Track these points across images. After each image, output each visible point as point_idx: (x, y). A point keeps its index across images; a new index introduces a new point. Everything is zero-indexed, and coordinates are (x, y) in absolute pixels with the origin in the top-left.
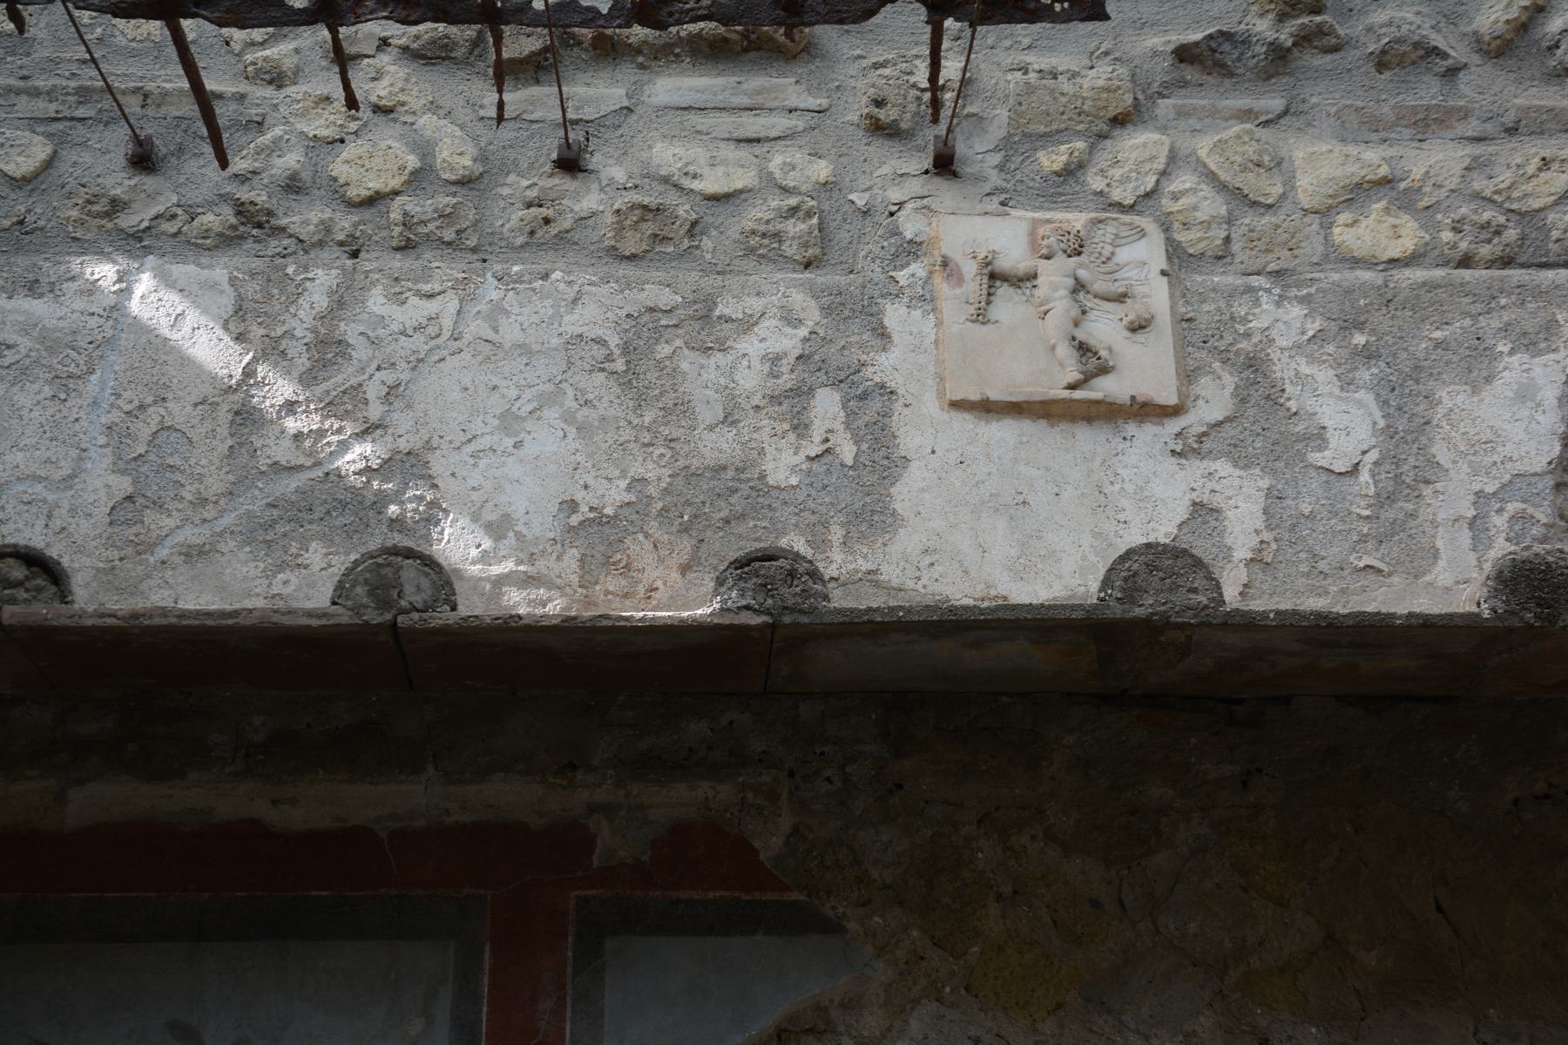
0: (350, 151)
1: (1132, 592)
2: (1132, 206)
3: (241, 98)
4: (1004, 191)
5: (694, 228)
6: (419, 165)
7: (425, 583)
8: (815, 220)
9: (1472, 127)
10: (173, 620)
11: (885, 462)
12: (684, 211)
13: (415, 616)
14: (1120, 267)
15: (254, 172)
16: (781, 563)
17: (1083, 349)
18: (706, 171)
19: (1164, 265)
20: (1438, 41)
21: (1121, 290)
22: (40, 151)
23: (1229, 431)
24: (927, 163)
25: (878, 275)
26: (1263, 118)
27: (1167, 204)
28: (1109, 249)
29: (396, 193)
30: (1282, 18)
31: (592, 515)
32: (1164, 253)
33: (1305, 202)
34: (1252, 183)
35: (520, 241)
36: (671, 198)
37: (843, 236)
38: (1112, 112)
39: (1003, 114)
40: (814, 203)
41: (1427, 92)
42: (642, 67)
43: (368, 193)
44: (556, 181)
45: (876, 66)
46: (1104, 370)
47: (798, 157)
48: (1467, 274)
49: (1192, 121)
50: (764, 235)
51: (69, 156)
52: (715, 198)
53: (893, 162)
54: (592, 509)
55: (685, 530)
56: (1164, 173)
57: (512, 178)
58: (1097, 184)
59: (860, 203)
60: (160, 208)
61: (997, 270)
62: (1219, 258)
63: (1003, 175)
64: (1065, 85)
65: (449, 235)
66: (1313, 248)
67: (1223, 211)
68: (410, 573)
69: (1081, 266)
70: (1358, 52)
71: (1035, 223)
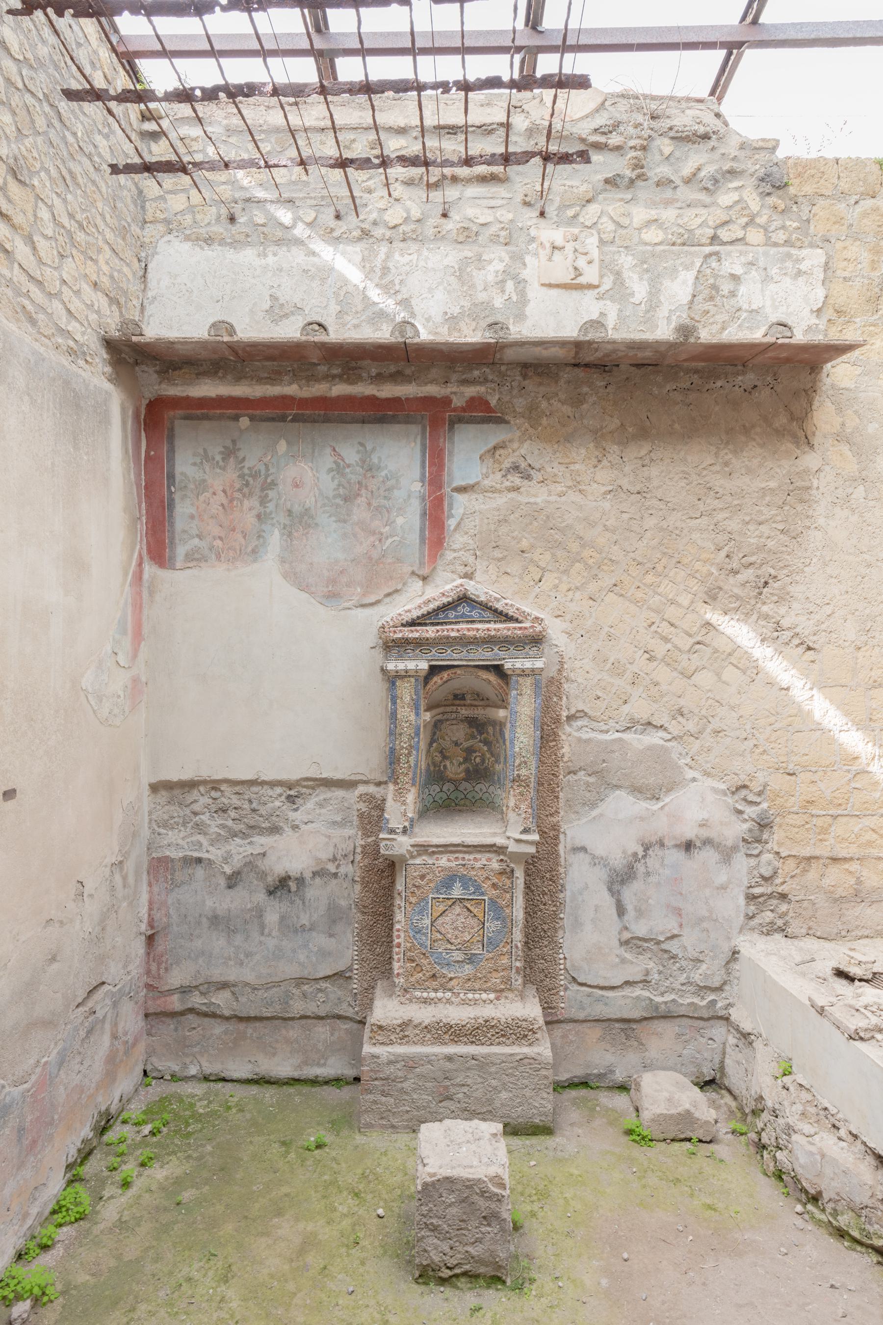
0: (389, 212)
3: (361, 197)
5: (477, 234)
9: (679, 205)
12: (475, 229)
17: (576, 269)
20: (673, 178)
22: (313, 215)
23: (611, 292)
24: (538, 214)
25: (524, 248)
30: (633, 170)
33: (635, 226)
36: (471, 225)
37: (515, 236)
39: (558, 199)
41: (668, 193)
45: (525, 184)
46: (580, 275)
47: (504, 212)
48: (674, 248)
51: (320, 216)
52: (482, 225)
55: (474, 320)
64: (575, 190)
65: (414, 237)
66: (636, 240)
71: (565, 232)
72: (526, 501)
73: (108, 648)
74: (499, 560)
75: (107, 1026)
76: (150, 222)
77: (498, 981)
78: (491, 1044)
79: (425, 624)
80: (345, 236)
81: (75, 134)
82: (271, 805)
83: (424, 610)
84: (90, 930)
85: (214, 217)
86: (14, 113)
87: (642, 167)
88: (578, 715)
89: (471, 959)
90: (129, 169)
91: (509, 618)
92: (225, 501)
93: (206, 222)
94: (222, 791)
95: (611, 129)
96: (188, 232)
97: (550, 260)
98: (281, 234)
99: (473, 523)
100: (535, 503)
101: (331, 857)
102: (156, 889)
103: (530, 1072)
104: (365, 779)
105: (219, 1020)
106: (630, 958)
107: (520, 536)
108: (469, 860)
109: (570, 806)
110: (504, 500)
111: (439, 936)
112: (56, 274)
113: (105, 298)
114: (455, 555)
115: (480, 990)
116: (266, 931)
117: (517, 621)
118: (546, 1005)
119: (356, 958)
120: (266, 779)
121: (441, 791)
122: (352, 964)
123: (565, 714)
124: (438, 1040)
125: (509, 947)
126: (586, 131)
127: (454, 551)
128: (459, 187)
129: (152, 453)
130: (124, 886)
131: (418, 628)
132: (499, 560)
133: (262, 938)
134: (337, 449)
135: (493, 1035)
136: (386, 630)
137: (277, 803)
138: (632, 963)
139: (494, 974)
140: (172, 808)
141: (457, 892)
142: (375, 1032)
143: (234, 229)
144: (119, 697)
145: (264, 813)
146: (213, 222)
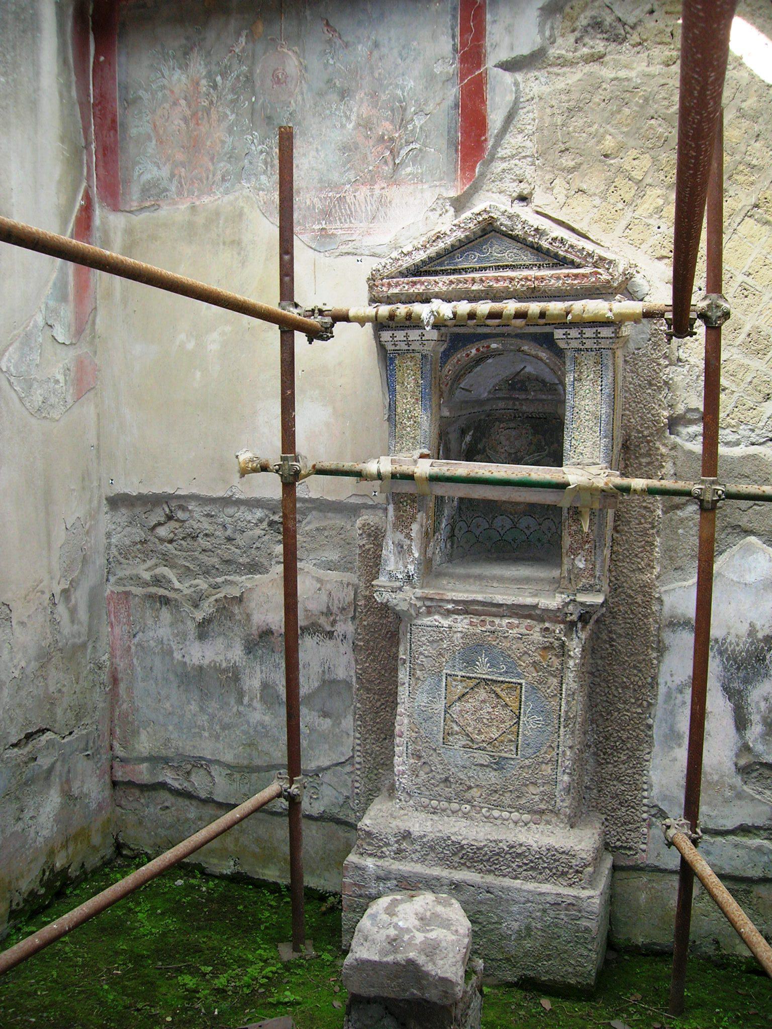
72: (612, 76)
73: (40, 319)
74: (571, 170)
75: (55, 779)
77: (537, 798)
78: (516, 878)
79: (436, 273)
82: (251, 533)
83: (432, 251)
84: (23, 664)
88: (689, 416)
89: (499, 764)
91: (562, 262)
92: (188, 113)
94: (190, 511)
99: (531, 115)
100: (628, 79)
101: (325, 610)
102: (117, 630)
103: (565, 919)
104: (371, 503)
105: (194, 802)
106: (751, 792)
107: (602, 130)
108: (500, 626)
109: (671, 558)
110: (579, 75)
111: (456, 728)
114: (505, 165)
115: (509, 806)
116: (246, 700)
117: (573, 264)
118: (618, 843)
119: (358, 748)
120: (242, 497)
121: (490, 528)
122: (353, 757)
123: (666, 413)
124: (444, 861)
125: (554, 753)
127: (503, 159)
129: (102, 58)
130: (73, 622)
131: (423, 279)
132: (571, 170)
133: (241, 708)
134: (331, 23)
135: (519, 866)
136: (378, 282)
137: (258, 532)
138: (753, 799)
139: (532, 789)
140: (134, 530)
141: (483, 670)
142: (362, 839)
144: (57, 382)
145: (241, 543)
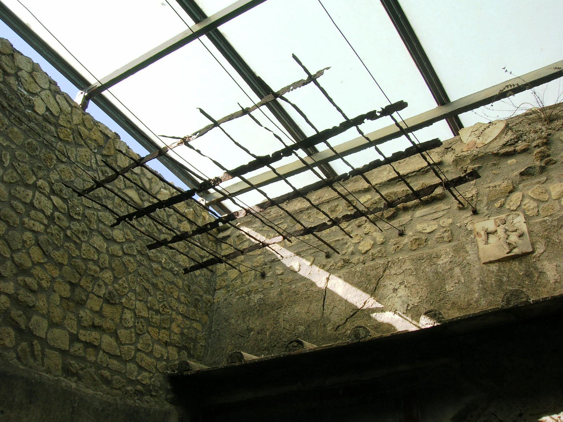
1: (508, 302)
2: (516, 210)
4: (489, 214)
5: (426, 240)
6: (373, 243)
7: (364, 332)
8: (450, 232)
10: (321, 349)
11: (471, 280)
12: (424, 238)
13: (363, 339)
14: (515, 224)
15: (346, 253)
16: (433, 312)
17: (509, 244)
18: (427, 228)
19: (524, 221)
21: (515, 229)
23: (546, 254)
24: (471, 213)
25: (464, 240)
26: (542, 182)
27: (523, 207)
28: (512, 220)
29: (370, 249)
30: (541, 160)
31: (412, 306)
32: (524, 218)
34: (541, 197)
35: (393, 253)
37: (456, 234)
38: (509, 191)
39: (486, 198)
40: (449, 228)
42: (413, 210)
43: (365, 251)
44: (399, 238)
46: (515, 248)
47: (445, 220)
49: (527, 187)
50: (440, 238)
53: (465, 215)
54: (412, 305)
55: (431, 304)
56: (522, 201)
57: (391, 240)
58: (508, 207)
59: (459, 225)
60: (331, 264)
61: (488, 232)
62: (537, 215)
63: (488, 211)
67: (536, 205)
68: (361, 331)
69: (506, 226)
70: (559, 163)
71: (495, 220)
76: (218, 290)
80: (333, 268)
81: (160, 262)
85: (253, 277)
86: (113, 270)
87: (549, 156)
90: (193, 269)
93: (248, 281)
95: (516, 140)
96: (237, 290)
97: (487, 243)
98: (292, 277)
112: (133, 347)
113: (175, 349)
126: (497, 148)
128: (410, 212)
143: (264, 282)
146: (253, 280)
